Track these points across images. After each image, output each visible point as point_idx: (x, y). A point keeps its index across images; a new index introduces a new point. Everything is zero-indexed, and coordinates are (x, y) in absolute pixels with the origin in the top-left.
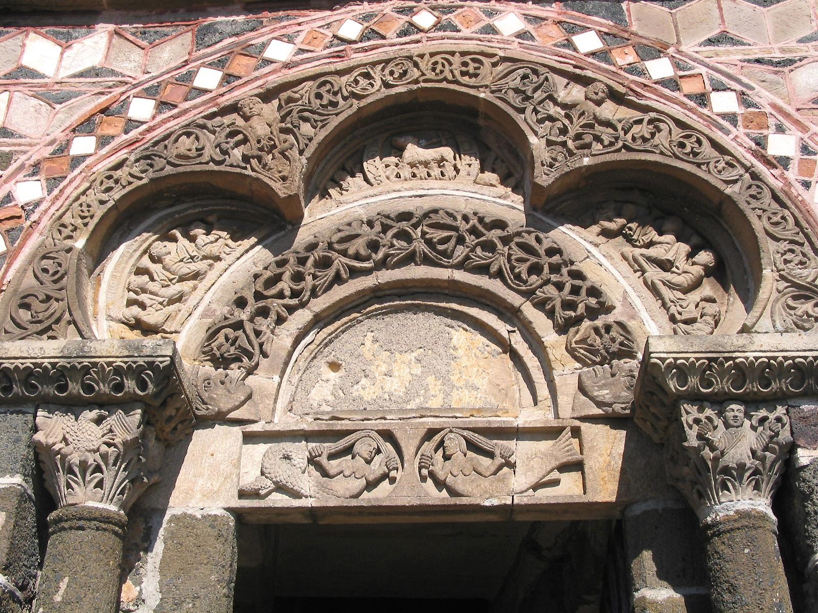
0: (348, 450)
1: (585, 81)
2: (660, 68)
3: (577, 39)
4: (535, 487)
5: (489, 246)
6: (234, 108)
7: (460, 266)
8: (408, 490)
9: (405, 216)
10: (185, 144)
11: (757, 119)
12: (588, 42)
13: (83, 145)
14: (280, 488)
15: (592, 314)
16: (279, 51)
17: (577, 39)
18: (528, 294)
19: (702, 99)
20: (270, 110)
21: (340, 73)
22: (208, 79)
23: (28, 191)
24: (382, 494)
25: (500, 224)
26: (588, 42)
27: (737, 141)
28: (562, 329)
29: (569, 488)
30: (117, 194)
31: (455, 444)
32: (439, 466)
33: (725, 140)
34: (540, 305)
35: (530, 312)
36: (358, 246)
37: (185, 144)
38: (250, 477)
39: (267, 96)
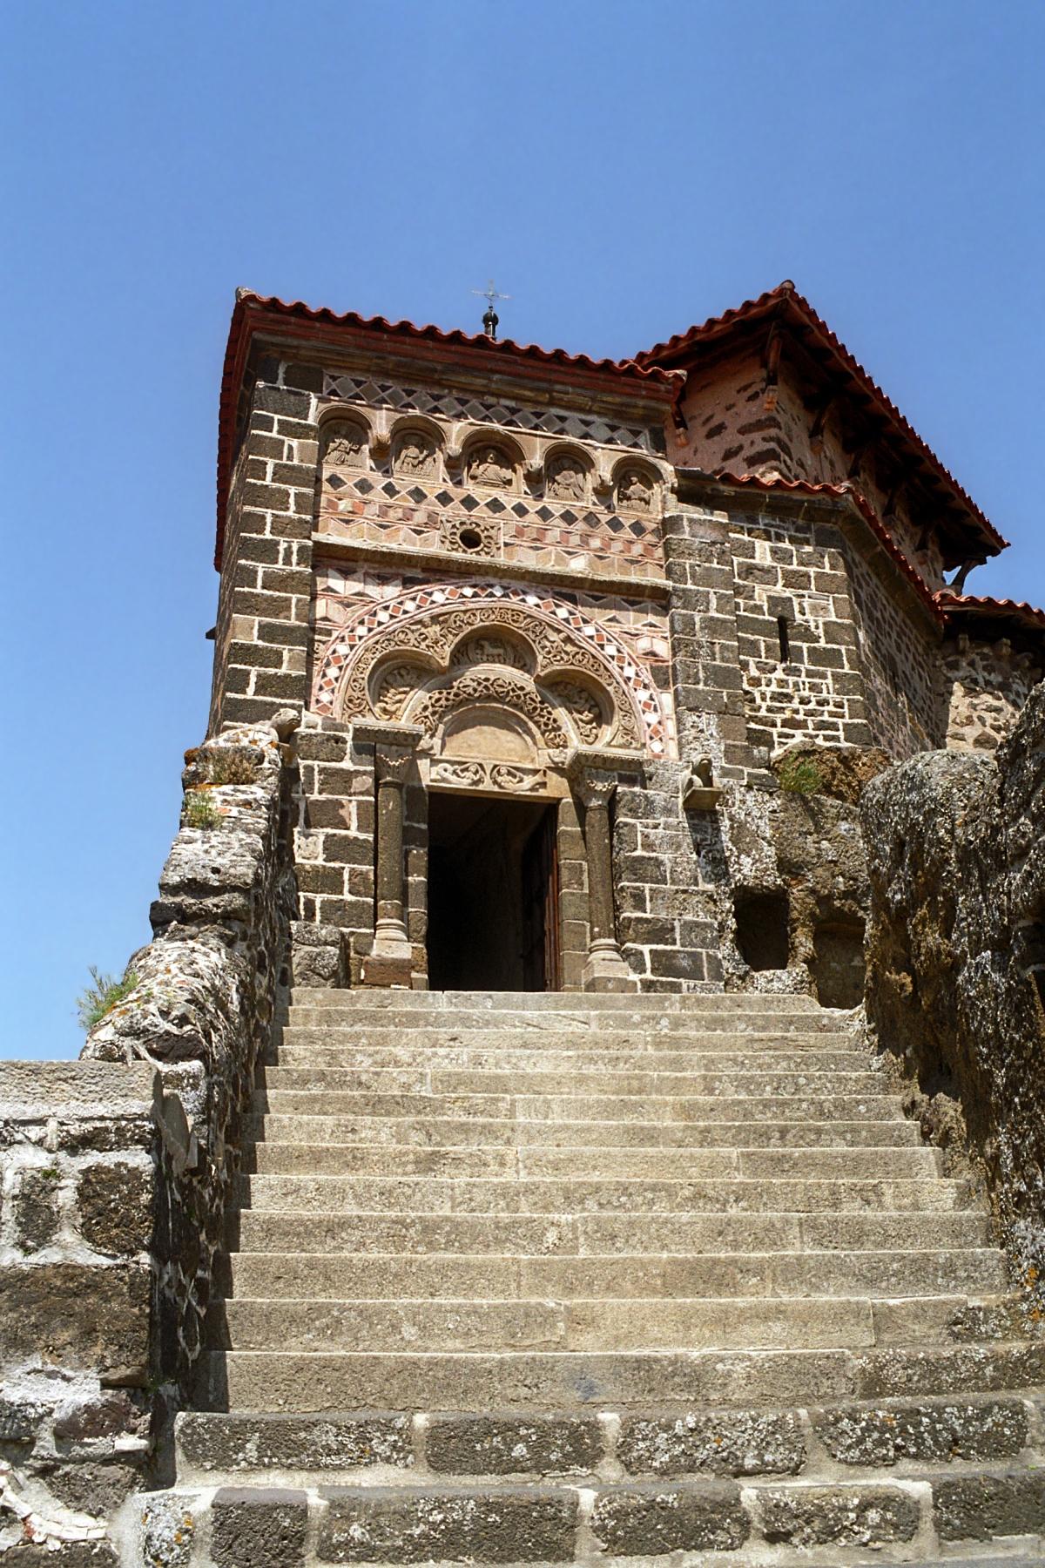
0: (466, 769)
1: (559, 631)
2: (589, 630)
3: (558, 611)
4: (532, 789)
5: (518, 697)
6: (420, 622)
7: (508, 704)
8: (487, 786)
9: (487, 680)
10: (402, 636)
11: (621, 659)
12: (562, 613)
13: (361, 631)
14: (444, 780)
15: (554, 729)
16: (439, 597)
17: (558, 611)
18: (531, 719)
19: (602, 646)
20: (437, 628)
21: (465, 612)
22: (410, 606)
23: (343, 649)
24: (480, 787)
25: (522, 688)
26: (562, 613)
27: (613, 666)
28: (543, 734)
29: (542, 792)
30: (378, 655)
31: (504, 770)
32: (499, 779)
33: (609, 666)
34: (536, 723)
35: (531, 724)
36: (470, 690)
37: (402, 636)
38: (433, 776)
39: (435, 619)
